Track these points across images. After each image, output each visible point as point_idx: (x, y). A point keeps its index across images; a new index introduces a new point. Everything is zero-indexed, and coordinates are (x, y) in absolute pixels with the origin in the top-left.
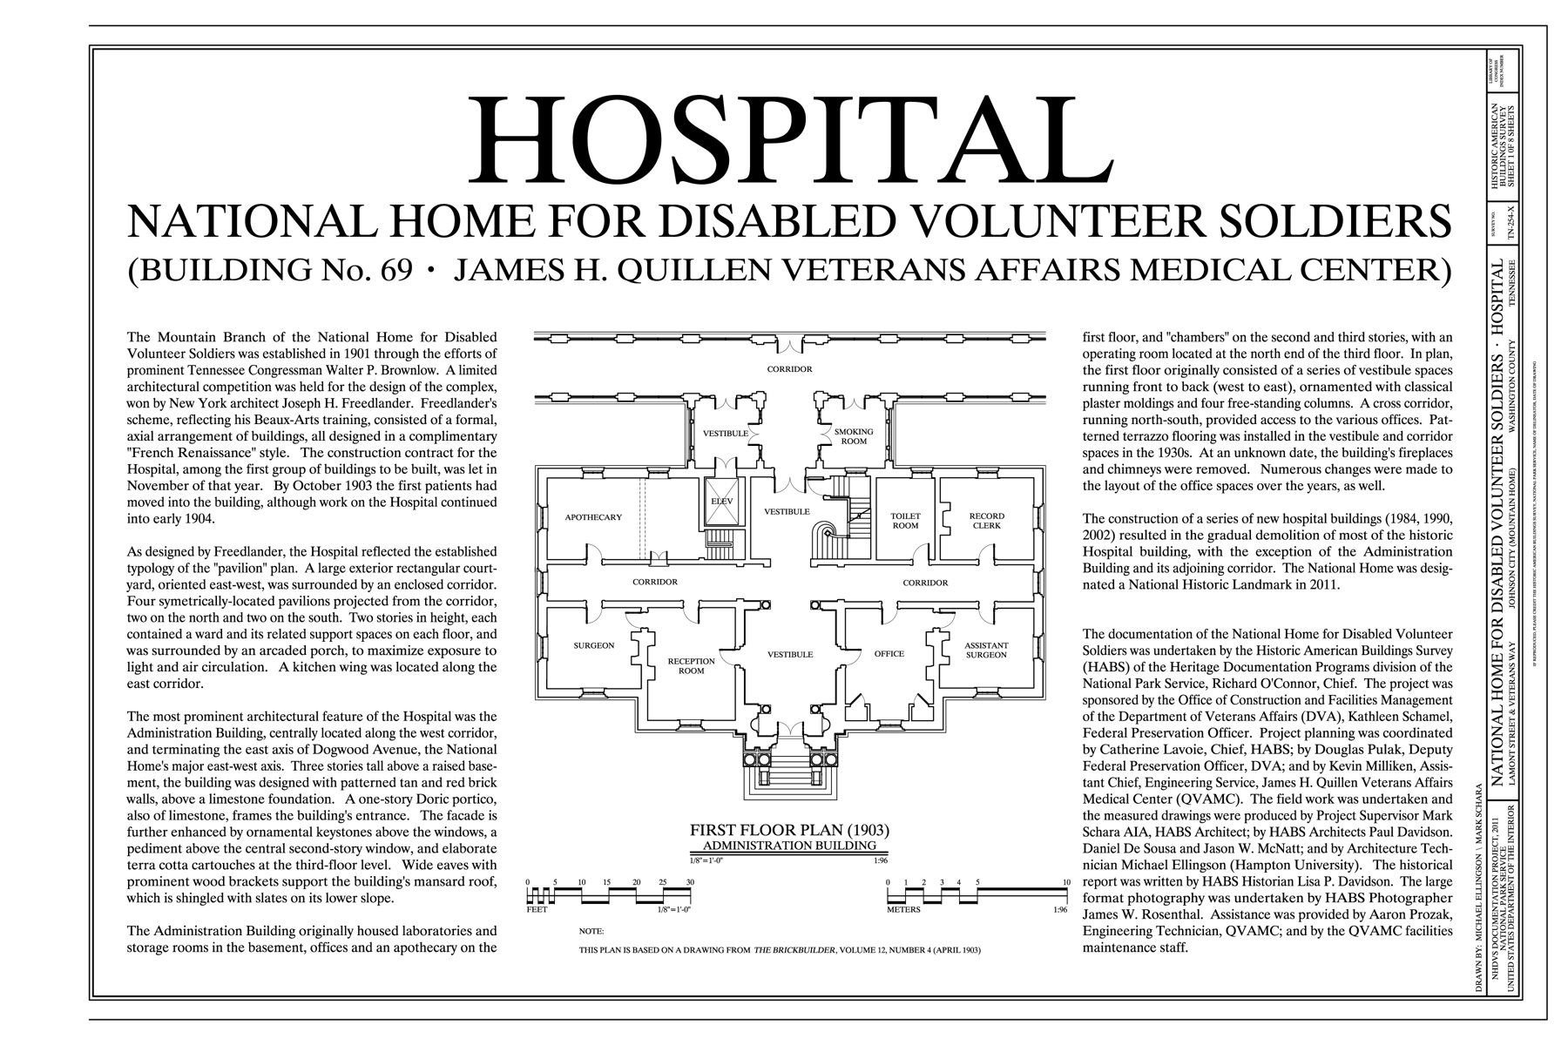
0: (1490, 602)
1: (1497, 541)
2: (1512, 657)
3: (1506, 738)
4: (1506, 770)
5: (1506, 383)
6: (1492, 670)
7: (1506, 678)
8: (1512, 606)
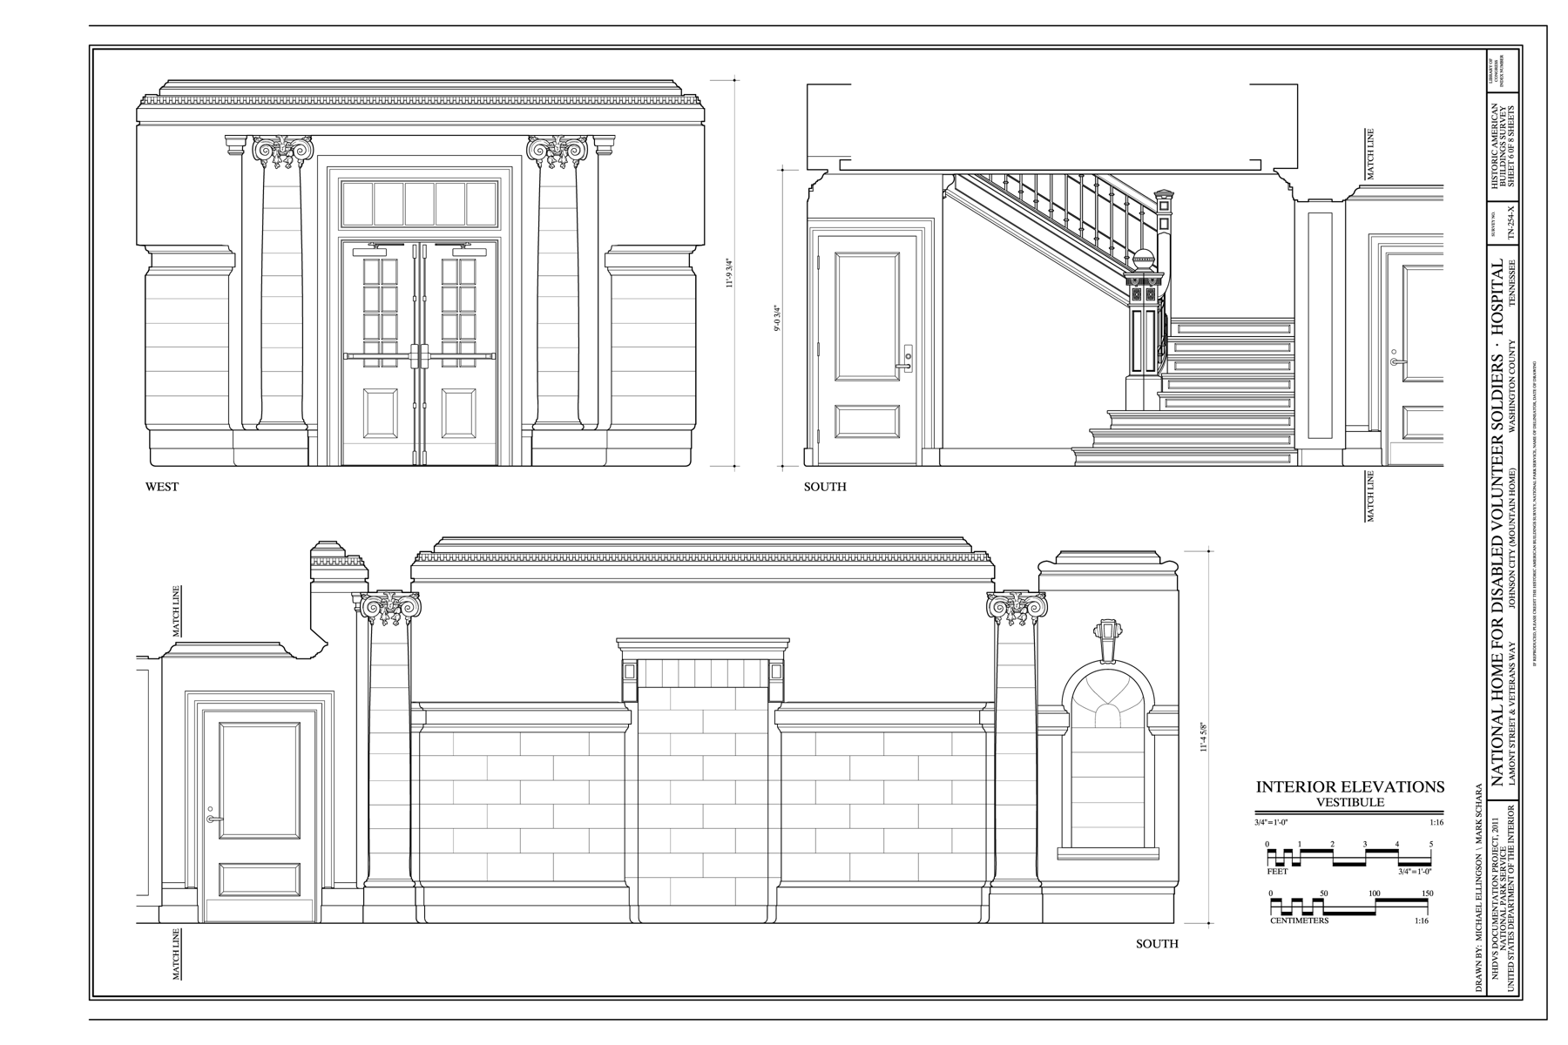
0: (1490, 602)
1: (1497, 541)
2: (1512, 657)
3: (1506, 738)
4: (1506, 770)
5: (1506, 383)
6: (1492, 670)
7: (1506, 678)
8: (1512, 606)
